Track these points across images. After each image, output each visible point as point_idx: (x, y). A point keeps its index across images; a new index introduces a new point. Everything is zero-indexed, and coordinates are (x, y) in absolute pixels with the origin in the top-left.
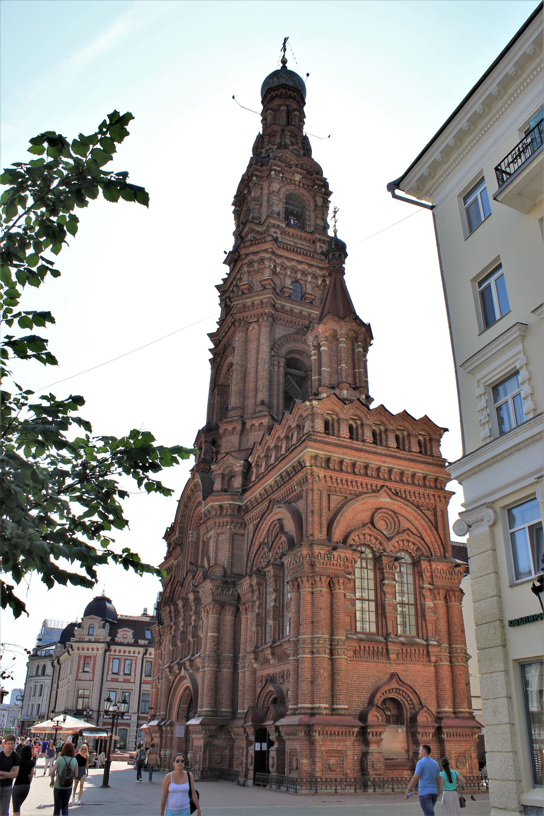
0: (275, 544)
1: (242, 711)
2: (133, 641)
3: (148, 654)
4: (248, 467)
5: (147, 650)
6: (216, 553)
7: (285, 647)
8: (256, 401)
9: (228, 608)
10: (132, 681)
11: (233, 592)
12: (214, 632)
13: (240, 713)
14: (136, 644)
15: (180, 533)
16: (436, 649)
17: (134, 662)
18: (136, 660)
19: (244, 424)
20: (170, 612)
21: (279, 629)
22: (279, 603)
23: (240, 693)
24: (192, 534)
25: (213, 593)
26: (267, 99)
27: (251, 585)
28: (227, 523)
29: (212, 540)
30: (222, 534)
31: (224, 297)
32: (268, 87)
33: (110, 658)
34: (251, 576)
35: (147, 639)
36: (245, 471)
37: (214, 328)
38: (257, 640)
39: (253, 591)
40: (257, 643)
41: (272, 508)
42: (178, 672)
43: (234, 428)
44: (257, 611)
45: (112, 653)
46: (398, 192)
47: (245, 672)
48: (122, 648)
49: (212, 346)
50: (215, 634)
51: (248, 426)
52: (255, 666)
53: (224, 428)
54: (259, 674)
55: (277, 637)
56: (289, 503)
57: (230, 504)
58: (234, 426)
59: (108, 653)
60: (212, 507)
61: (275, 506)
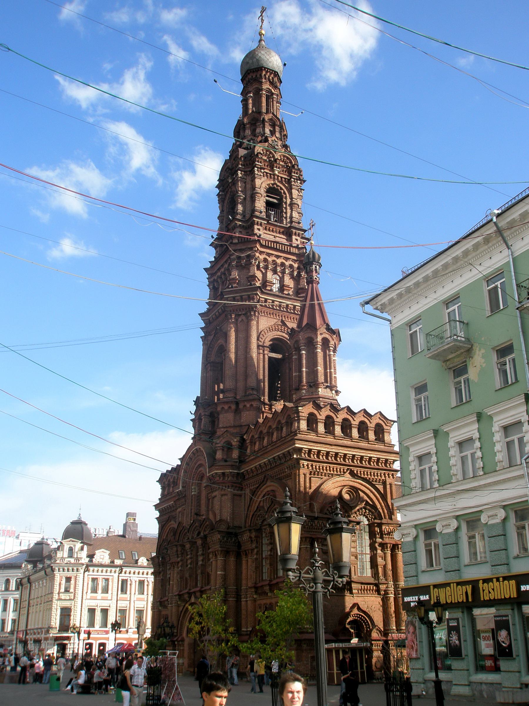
0: (270, 509)
1: (245, 629)
2: (109, 561)
3: (123, 572)
4: (243, 441)
5: (122, 570)
6: (221, 510)
7: (280, 585)
8: (246, 384)
9: (231, 553)
10: (110, 598)
11: (235, 540)
12: (221, 571)
13: (244, 631)
14: (112, 565)
15: (183, 487)
16: (385, 586)
17: (110, 581)
18: (113, 579)
19: (237, 404)
20: (177, 551)
21: (274, 572)
22: (274, 553)
23: (243, 617)
24: (195, 489)
25: (221, 542)
26: (247, 79)
27: (251, 537)
28: (229, 487)
29: (216, 499)
30: (225, 495)
31: (212, 279)
32: (246, 68)
33: (88, 578)
34: (250, 530)
35: (122, 559)
36: (240, 444)
37: (204, 308)
38: (256, 578)
39: (252, 541)
40: (256, 580)
41: (267, 481)
42: (188, 599)
43: (230, 407)
44: (255, 556)
45: (91, 573)
46: (369, 308)
47: (247, 601)
48: (100, 569)
49: (203, 325)
50: (223, 573)
51: (241, 406)
52: (255, 596)
53: (221, 407)
54: (258, 602)
55: (272, 577)
56: (280, 479)
57: (231, 472)
58: (229, 405)
59: (87, 573)
60: (216, 473)
61: (269, 481)
